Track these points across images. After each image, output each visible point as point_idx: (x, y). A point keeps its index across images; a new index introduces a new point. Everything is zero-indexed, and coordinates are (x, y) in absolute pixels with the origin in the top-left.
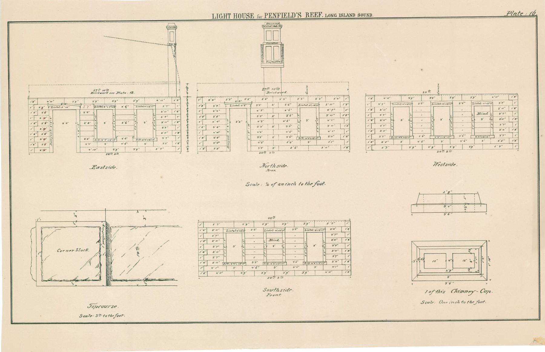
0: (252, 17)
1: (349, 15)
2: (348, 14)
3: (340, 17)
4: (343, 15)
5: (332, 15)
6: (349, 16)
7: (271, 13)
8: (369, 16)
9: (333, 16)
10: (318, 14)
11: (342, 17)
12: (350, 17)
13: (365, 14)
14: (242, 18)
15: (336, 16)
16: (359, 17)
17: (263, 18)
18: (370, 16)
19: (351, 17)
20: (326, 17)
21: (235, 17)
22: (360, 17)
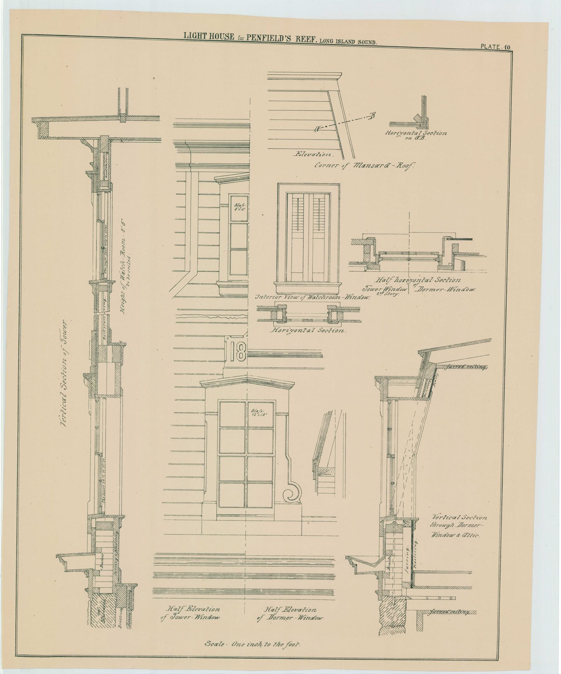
2: (346, 40)
3: (337, 43)
4: (341, 41)
5: (328, 40)
6: (347, 43)
7: (305, 36)
8: (372, 43)
9: (328, 42)
11: (339, 44)
12: (349, 43)
13: (367, 41)
15: (332, 42)
16: (359, 44)
18: (373, 44)
19: (350, 44)
20: (320, 42)
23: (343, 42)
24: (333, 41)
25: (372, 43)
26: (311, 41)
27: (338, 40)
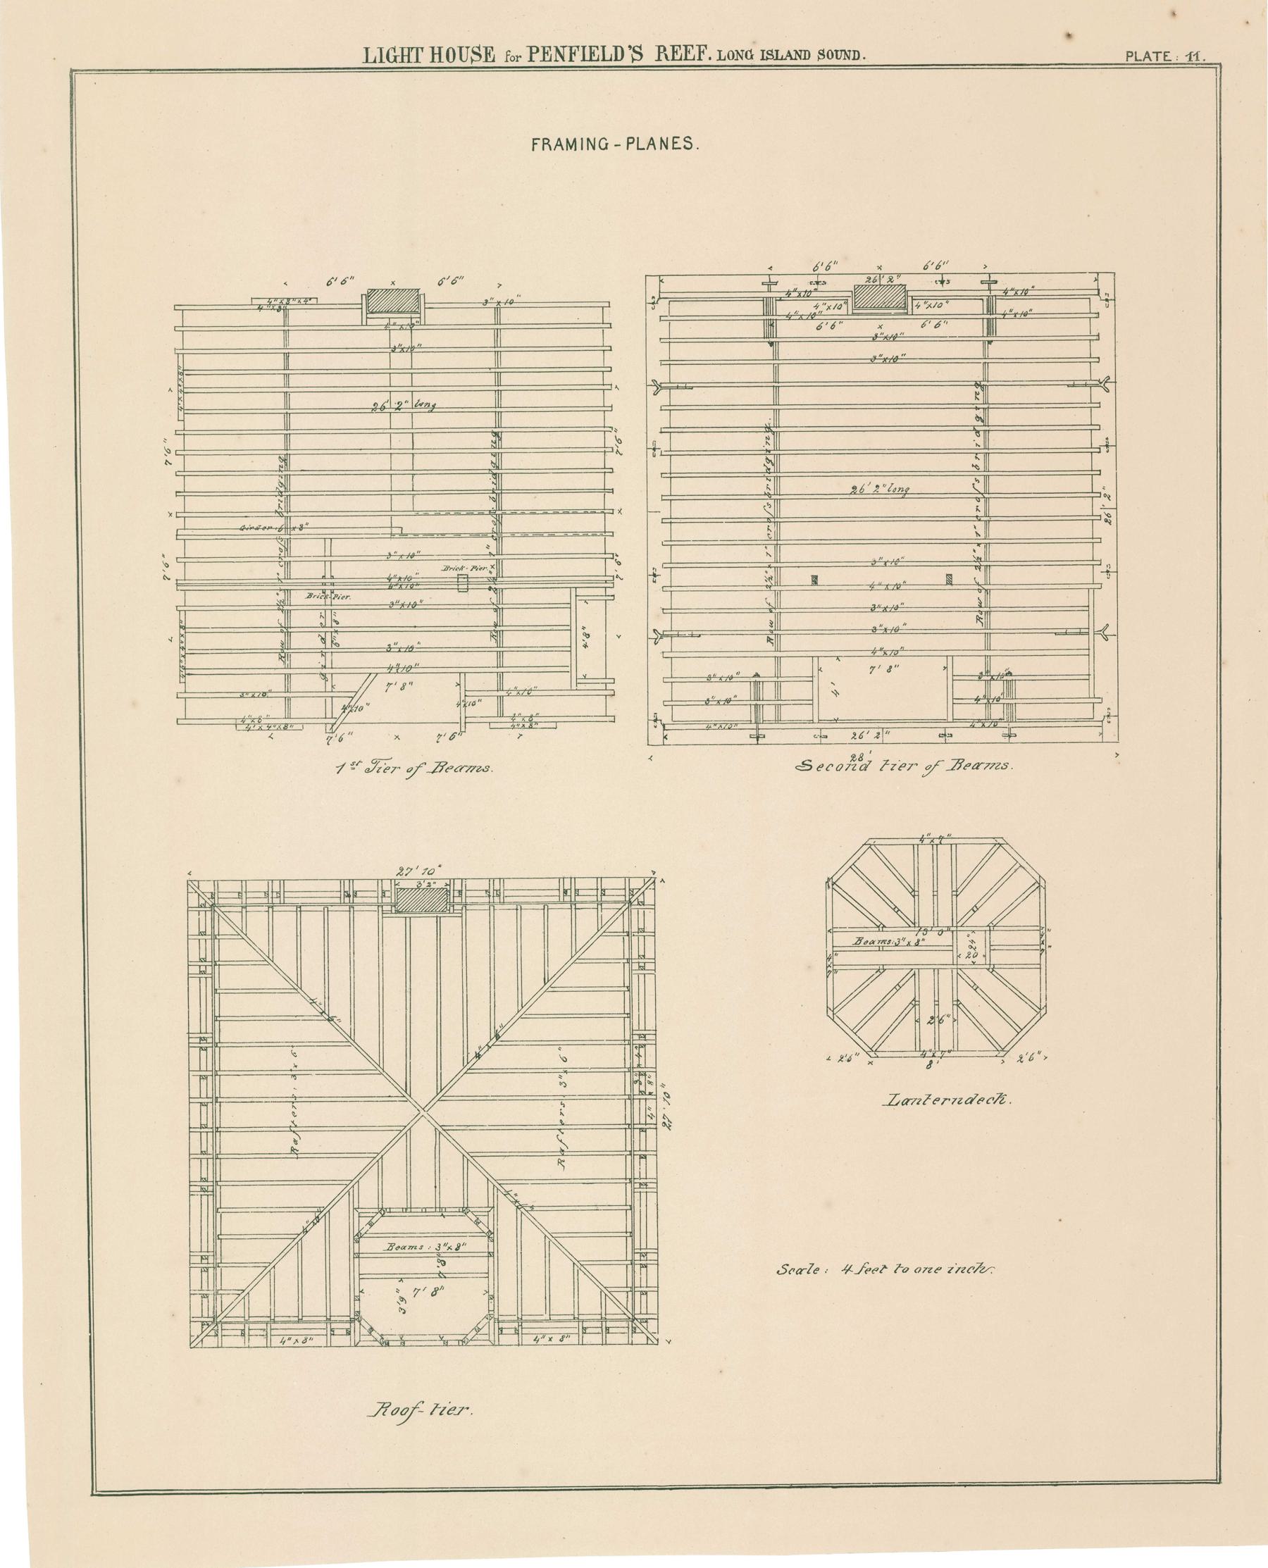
0: (490, 59)
1: (793, 54)
2: (789, 52)
5: (741, 53)
8: (852, 57)
10: (694, 52)
12: (796, 59)
13: (839, 53)
14: (457, 63)
15: (752, 57)
17: (524, 62)
20: (720, 59)
21: (437, 57)
22: (826, 61)
23: (780, 57)
24: (752, 56)
25: (852, 57)
26: (697, 58)
27: (765, 52)
